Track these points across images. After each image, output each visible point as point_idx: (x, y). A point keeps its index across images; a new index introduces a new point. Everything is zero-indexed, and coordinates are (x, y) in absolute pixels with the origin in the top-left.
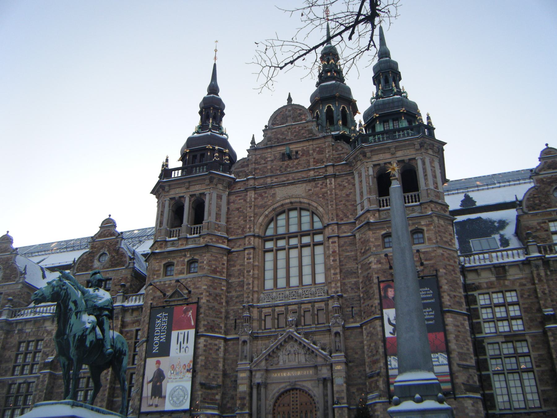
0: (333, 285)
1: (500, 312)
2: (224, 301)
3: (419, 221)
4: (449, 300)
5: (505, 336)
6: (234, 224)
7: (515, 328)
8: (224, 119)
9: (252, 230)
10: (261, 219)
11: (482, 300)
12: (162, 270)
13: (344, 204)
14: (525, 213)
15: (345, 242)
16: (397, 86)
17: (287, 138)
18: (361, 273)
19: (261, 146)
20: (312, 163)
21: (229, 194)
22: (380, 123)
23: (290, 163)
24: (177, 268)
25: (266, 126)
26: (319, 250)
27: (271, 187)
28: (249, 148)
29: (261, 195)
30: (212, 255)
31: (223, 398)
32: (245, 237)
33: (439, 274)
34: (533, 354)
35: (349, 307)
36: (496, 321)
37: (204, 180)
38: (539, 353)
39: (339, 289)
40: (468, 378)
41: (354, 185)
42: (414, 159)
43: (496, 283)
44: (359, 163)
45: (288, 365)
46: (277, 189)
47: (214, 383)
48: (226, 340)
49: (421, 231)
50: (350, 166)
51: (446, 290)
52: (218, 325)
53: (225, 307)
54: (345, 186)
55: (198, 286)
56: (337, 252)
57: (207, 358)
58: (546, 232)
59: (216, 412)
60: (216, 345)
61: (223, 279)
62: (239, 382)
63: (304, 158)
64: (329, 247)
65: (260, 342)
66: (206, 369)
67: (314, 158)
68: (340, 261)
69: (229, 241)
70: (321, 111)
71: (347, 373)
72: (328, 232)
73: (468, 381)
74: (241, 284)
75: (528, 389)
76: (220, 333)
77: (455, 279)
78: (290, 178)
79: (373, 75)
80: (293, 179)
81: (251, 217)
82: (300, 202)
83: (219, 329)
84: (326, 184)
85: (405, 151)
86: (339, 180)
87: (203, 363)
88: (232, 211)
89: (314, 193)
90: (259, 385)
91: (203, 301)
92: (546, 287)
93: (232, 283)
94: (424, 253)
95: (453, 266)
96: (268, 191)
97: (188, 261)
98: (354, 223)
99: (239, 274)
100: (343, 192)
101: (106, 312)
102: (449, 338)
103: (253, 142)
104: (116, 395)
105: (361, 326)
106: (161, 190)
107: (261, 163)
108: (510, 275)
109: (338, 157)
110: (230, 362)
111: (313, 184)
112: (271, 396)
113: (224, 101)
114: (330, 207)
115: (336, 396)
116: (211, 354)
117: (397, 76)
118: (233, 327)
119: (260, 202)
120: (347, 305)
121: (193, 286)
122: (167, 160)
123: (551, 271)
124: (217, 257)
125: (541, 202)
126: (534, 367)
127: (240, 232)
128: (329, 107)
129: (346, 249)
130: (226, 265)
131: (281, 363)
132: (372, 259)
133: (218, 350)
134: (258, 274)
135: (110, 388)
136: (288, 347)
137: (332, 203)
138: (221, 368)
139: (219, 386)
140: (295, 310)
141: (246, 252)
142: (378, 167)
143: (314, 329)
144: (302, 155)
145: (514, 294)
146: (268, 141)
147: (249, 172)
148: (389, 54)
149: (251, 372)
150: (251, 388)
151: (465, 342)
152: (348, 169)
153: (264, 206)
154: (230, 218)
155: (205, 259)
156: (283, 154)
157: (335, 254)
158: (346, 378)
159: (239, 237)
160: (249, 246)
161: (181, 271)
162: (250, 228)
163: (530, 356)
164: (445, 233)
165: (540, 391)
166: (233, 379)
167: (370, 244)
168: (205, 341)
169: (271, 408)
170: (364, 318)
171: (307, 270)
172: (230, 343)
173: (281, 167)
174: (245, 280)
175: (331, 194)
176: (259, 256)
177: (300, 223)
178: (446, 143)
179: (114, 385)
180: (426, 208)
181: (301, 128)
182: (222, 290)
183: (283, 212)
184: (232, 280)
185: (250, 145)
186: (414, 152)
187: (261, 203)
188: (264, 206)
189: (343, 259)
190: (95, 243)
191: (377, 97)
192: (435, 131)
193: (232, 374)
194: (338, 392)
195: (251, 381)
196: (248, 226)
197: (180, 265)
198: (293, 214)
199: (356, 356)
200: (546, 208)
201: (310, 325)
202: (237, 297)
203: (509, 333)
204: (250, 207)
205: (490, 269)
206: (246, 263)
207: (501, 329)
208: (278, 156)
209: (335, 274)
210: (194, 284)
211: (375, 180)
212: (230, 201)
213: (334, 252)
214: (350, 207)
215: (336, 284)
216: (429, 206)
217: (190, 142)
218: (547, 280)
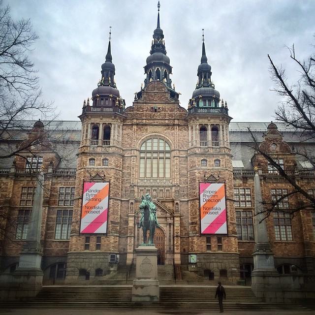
2: (121, 181)
5: (244, 209)
7: (248, 206)
12: (88, 162)
23: (156, 114)
24: (97, 162)
27: (146, 125)
31: (120, 228)
37: (111, 116)
39: (178, 183)
44: (192, 121)
48: (121, 201)
57: (114, 209)
66: (113, 214)
70: (153, 70)
72: (174, 153)
82: (160, 136)
96: (144, 127)
98: (187, 151)
105: (188, 201)
132: (196, 171)
139: (117, 223)
141: (132, 158)
142: (201, 125)
143: (165, 200)
145: (249, 190)
149: (135, 218)
156: (152, 108)
159: (128, 149)
168: (113, 201)
171: (161, 171)
175: (176, 134)
184: (124, 171)
194: (176, 230)
198: (155, 141)
199: (184, 214)
207: (242, 206)
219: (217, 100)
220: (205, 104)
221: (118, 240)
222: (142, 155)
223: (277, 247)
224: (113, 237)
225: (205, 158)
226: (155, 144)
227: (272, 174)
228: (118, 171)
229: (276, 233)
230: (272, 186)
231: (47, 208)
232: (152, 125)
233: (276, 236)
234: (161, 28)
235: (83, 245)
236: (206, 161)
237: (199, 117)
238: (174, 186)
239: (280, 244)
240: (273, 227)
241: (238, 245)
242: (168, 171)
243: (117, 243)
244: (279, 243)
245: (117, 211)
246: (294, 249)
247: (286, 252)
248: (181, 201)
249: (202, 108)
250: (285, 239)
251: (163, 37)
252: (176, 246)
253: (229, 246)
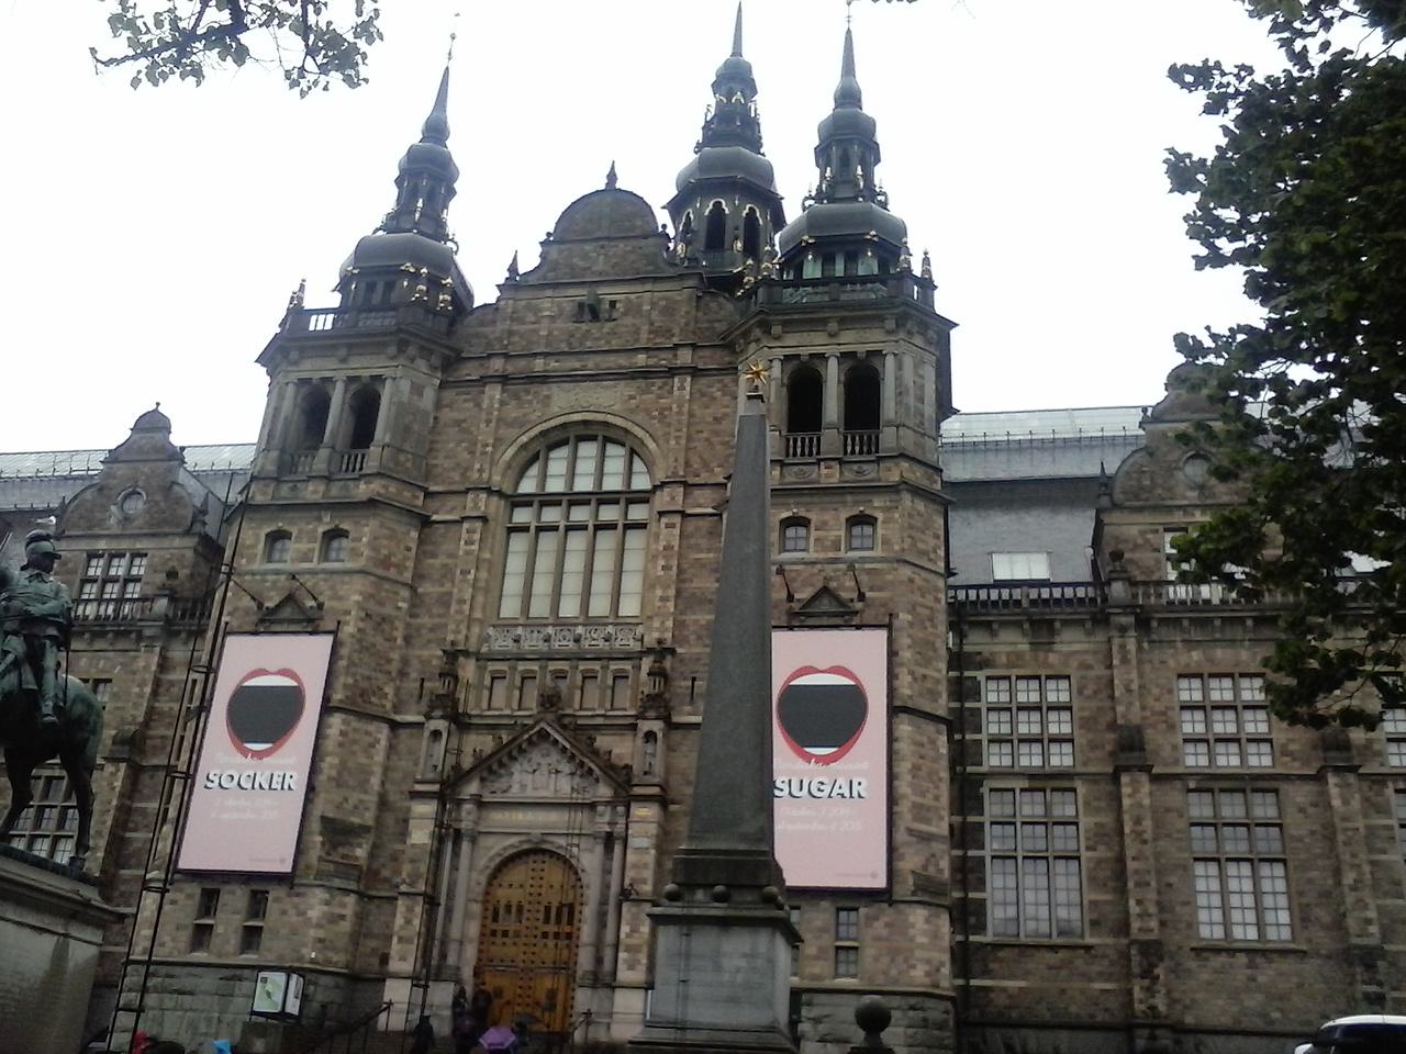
0: (656, 624)
1: (1028, 725)
2: (399, 635)
3: (869, 497)
4: (911, 687)
6: (446, 457)
7: (1055, 761)
8: (452, 204)
9: (485, 476)
10: (510, 452)
11: (993, 694)
12: (261, 546)
13: (707, 440)
15: (698, 529)
16: (868, 176)
17: (594, 269)
19: (532, 280)
20: (644, 336)
21: (443, 386)
22: (815, 259)
23: (594, 328)
24: (293, 547)
25: (549, 234)
26: (635, 540)
27: (544, 379)
28: (502, 281)
29: (518, 398)
30: (382, 525)
31: (372, 856)
32: (468, 490)
33: (896, 623)
34: (1084, 821)
35: (685, 679)
36: (1016, 742)
37: (385, 345)
38: (1098, 820)
39: (668, 635)
40: (928, 861)
43: (1028, 657)
44: (753, 347)
45: (530, 794)
48: (395, 726)
49: (870, 521)
50: (734, 352)
51: (905, 660)
53: (400, 648)
54: (715, 399)
55: (341, 593)
56: (676, 548)
57: (343, 763)
58: (1156, 555)
59: (353, 886)
60: (367, 733)
61: (406, 584)
62: (411, 822)
63: (629, 320)
64: (657, 536)
66: (338, 786)
67: (652, 324)
68: (680, 571)
69: (428, 494)
71: (661, 826)
72: (662, 500)
73: (925, 867)
74: (445, 601)
75: (1061, 897)
77: (931, 638)
78: (590, 364)
79: (816, 142)
80: (597, 367)
81: (487, 445)
82: (606, 424)
83: (380, 698)
85: (862, 333)
86: (704, 381)
87: (334, 773)
88: (445, 425)
89: (642, 406)
91: (349, 629)
92: (1134, 675)
93: (423, 594)
94: (870, 572)
95: (931, 608)
96: (534, 388)
97: (324, 533)
99: (444, 576)
100: (708, 411)
101: (52, 631)
102: (896, 770)
103: (513, 269)
104: (131, 825)
106: (279, 356)
107: (527, 319)
108: (1062, 643)
109: (707, 329)
110: (397, 775)
111: (641, 383)
112: (482, 862)
113: (458, 159)
115: (630, 874)
116: (354, 753)
117: (871, 155)
118: (416, 698)
119: (512, 412)
120: (682, 673)
121: (328, 593)
122: (302, 287)
123: (1151, 642)
124: (393, 530)
125: (1154, 485)
126: (1083, 849)
127: (457, 479)
128: (718, 205)
129: (698, 545)
130: (414, 551)
131: (515, 789)
134: (487, 581)
135: (118, 809)
136: (536, 755)
137: (678, 434)
140: (561, 671)
141: (466, 525)
142: (795, 362)
143: (600, 721)
144: (625, 314)
145: (1064, 684)
146: (549, 271)
147: (496, 338)
148: (860, 100)
151: (933, 783)
152: (727, 359)
153: (521, 424)
154: (437, 442)
155: (365, 533)
156: (581, 305)
157: (669, 553)
158: (657, 836)
160: (475, 514)
161: (306, 554)
162: (481, 471)
163: (1076, 824)
164: (923, 532)
165: (1085, 902)
166: (401, 816)
168: (344, 722)
169: (480, 889)
172: (404, 733)
173: (573, 336)
174: (455, 591)
175: (680, 413)
176: (494, 538)
177: (600, 474)
178: (956, 325)
179: (128, 803)
180: (889, 470)
181: (629, 248)
182: (399, 608)
185: (507, 275)
187: (514, 415)
188: (521, 424)
189: (686, 566)
190: (116, 466)
191: (820, 196)
192: (936, 292)
193: (399, 804)
194: (635, 866)
196: (477, 466)
197: (305, 540)
198: (588, 450)
200: (1163, 499)
201: (594, 710)
202: (432, 630)
204: (488, 422)
205: (1018, 624)
206: (461, 553)
207: (1024, 761)
208: (568, 307)
209: (664, 599)
210: (332, 588)
211: (785, 389)
212: (444, 402)
213: (668, 548)
214: (718, 447)
215: (663, 623)
216: (897, 465)
217: (364, 250)
218: (1140, 662)
221: (349, 911)
222: (522, 516)
223: (1205, 976)
224: (321, 894)
225: (803, 513)
226: (586, 466)
227: (1194, 602)
228: (387, 586)
229: (1202, 900)
230: (1183, 659)
231: (123, 766)
233: (1203, 916)
234: (748, 55)
235: (185, 927)
237: (785, 323)
238: (649, 651)
239: (1223, 959)
240: (1185, 868)
242: (632, 583)
243: (346, 926)
244: (1217, 950)
245: (365, 772)
246: (1300, 986)
247: (1253, 1001)
250: (1252, 934)
251: (750, 88)
252: (629, 949)
253: (894, 954)
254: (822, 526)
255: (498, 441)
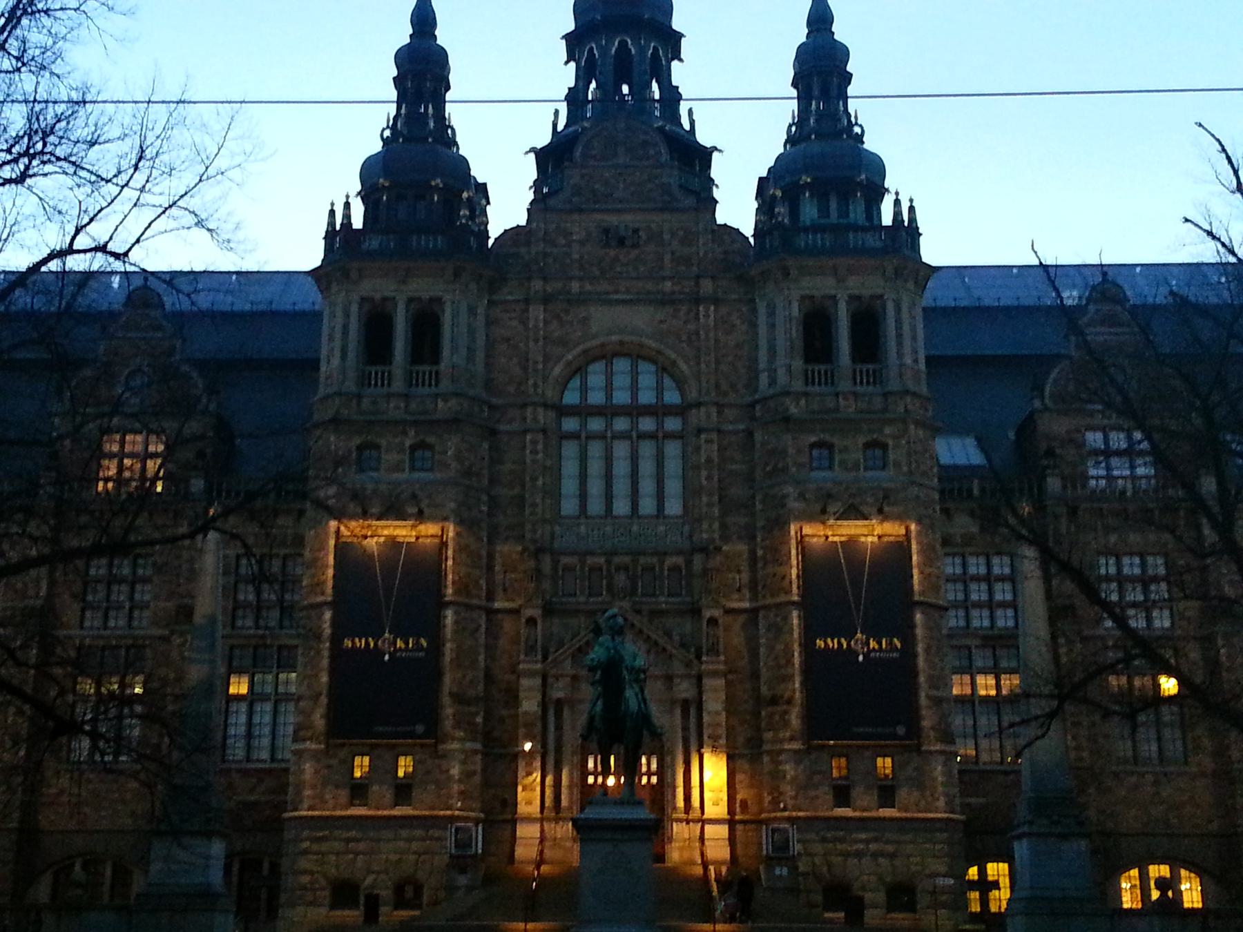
0: (705, 526)
1: (978, 593)
5: (984, 638)
7: (1000, 623)
9: (540, 391)
10: (557, 370)
14: (1046, 409)
18: (762, 510)
21: (491, 303)
22: (811, 196)
27: (582, 300)
29: (558, 317)
39: (716, 536)
41: (754, 325)
42: (881, 296)
46: (592, 309)
47: (471, 693)
49: (884, 447)
52: (477, 582)
59: (478, 746)
65: (556, 621)
67: (673, 253)
69: (492, 407)
72: (697, 417)
74: (520, 502)
76: (479, 597)
84: (698, 314)
86: (724, 310)
90: (559, 703)
97: (411, 446)
105: (754, 612)
114: (703, 366)
128: (623, 44)
133: (477, 630)
138: (482, 664)
141: (528, 437)
150: (544, 705)
156: (606, 231)
162: (535, 385)
167: (789, 460)
170: (764, 597)
171: (647, 486)
182: (481, 512)
183: (603, 357)
186: (882, 283)
188: (564, 343)
195: (544, 695)
198: (621, 365)
203: (990, 633)
204: (536, 341)
206: (528, 461)
207: (976, 623)
209: (710, 505)
210: (429, 496)
213: (709, 460)
219: (876, 191)
220: (824, 211)
221: (479, 768)
222: (570, 424)
225: (826, 437)
226: (622, 380)
232: (610, 303)
236: (830, 447)
241: (961, 782)
243: (477, 779)
248: (729, 612)
249: (815, 228)
254: (845, 449)
255: (547, 358)
